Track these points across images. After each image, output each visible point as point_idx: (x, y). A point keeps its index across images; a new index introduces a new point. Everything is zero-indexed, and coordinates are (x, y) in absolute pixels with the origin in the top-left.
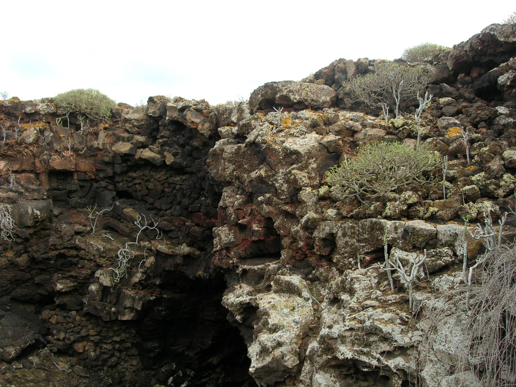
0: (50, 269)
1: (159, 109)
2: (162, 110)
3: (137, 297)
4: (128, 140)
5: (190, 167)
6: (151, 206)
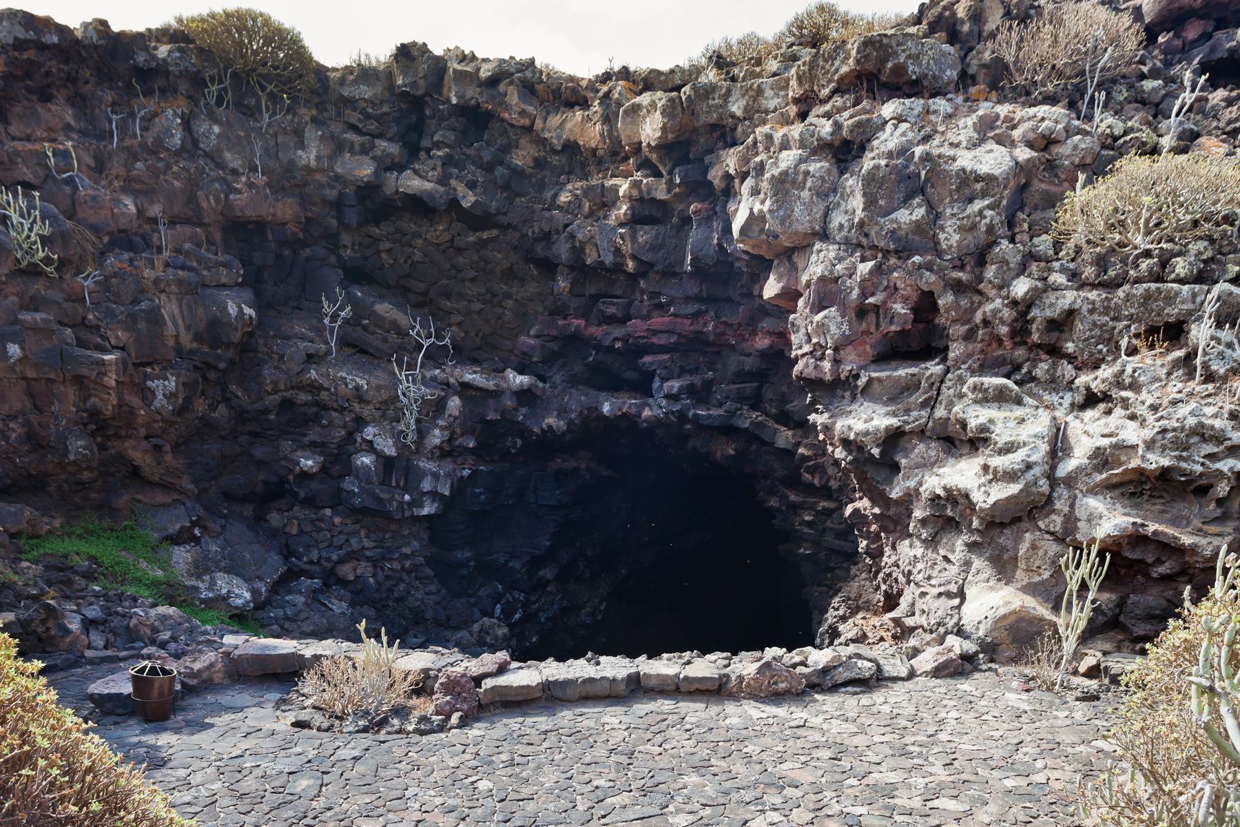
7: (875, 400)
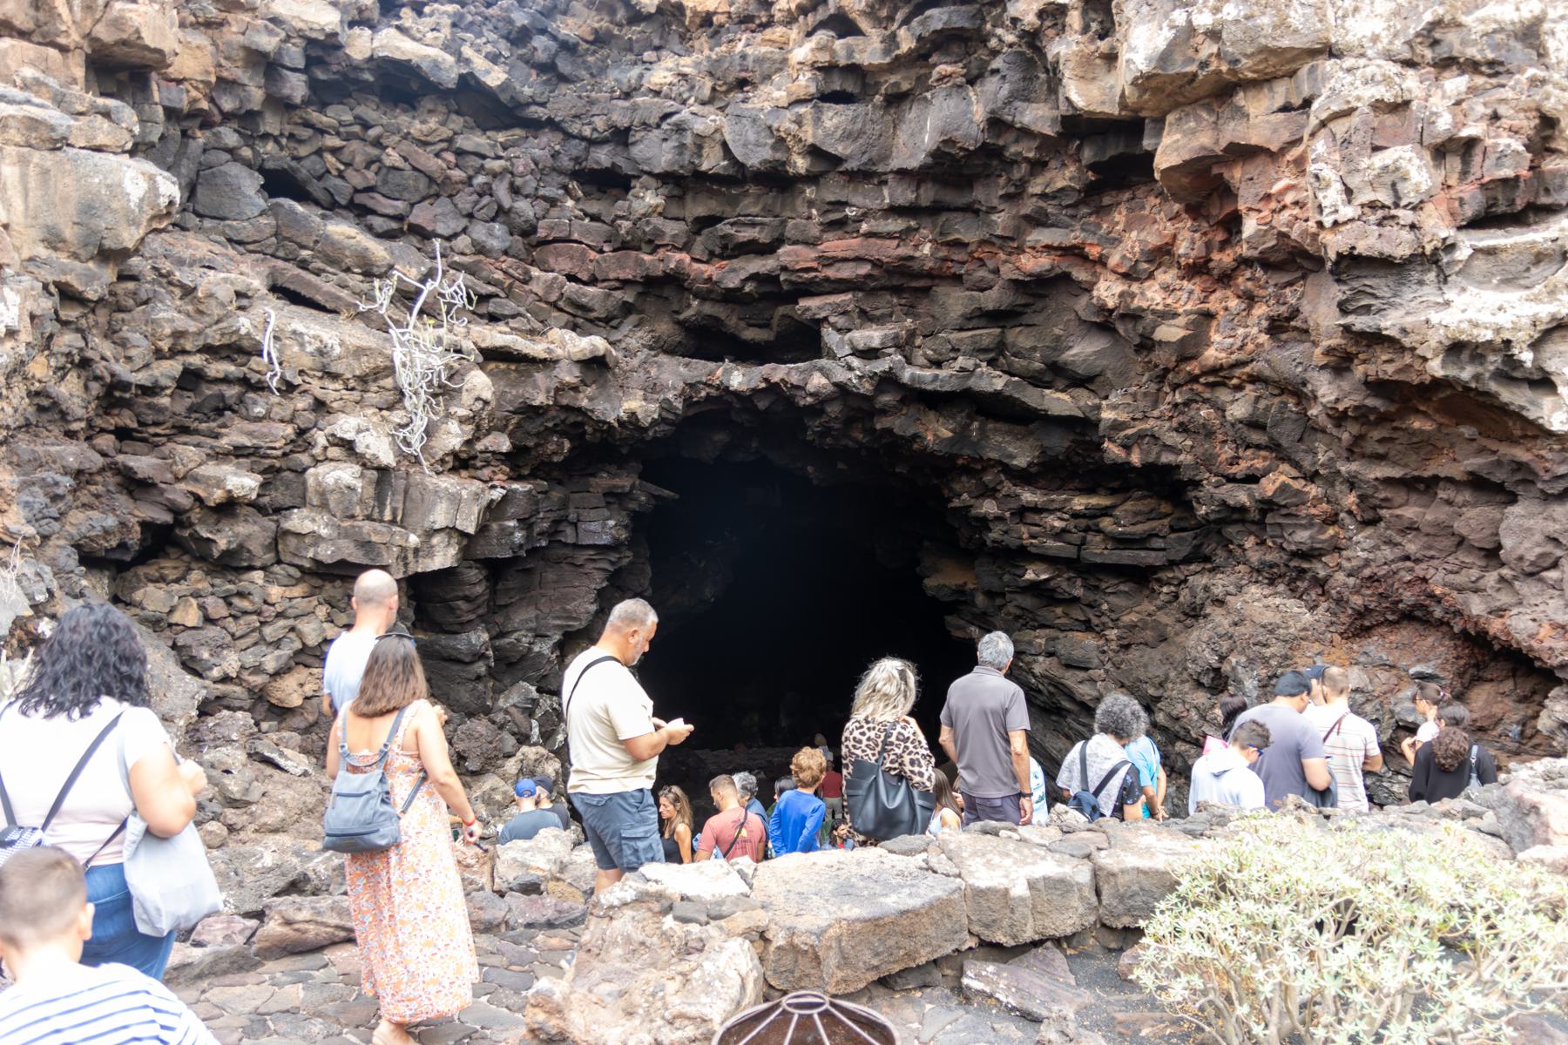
0: (152, 430)
3: (464, 493)
5: (543, 105)
6: (394, 225)
7: (1483, 282)
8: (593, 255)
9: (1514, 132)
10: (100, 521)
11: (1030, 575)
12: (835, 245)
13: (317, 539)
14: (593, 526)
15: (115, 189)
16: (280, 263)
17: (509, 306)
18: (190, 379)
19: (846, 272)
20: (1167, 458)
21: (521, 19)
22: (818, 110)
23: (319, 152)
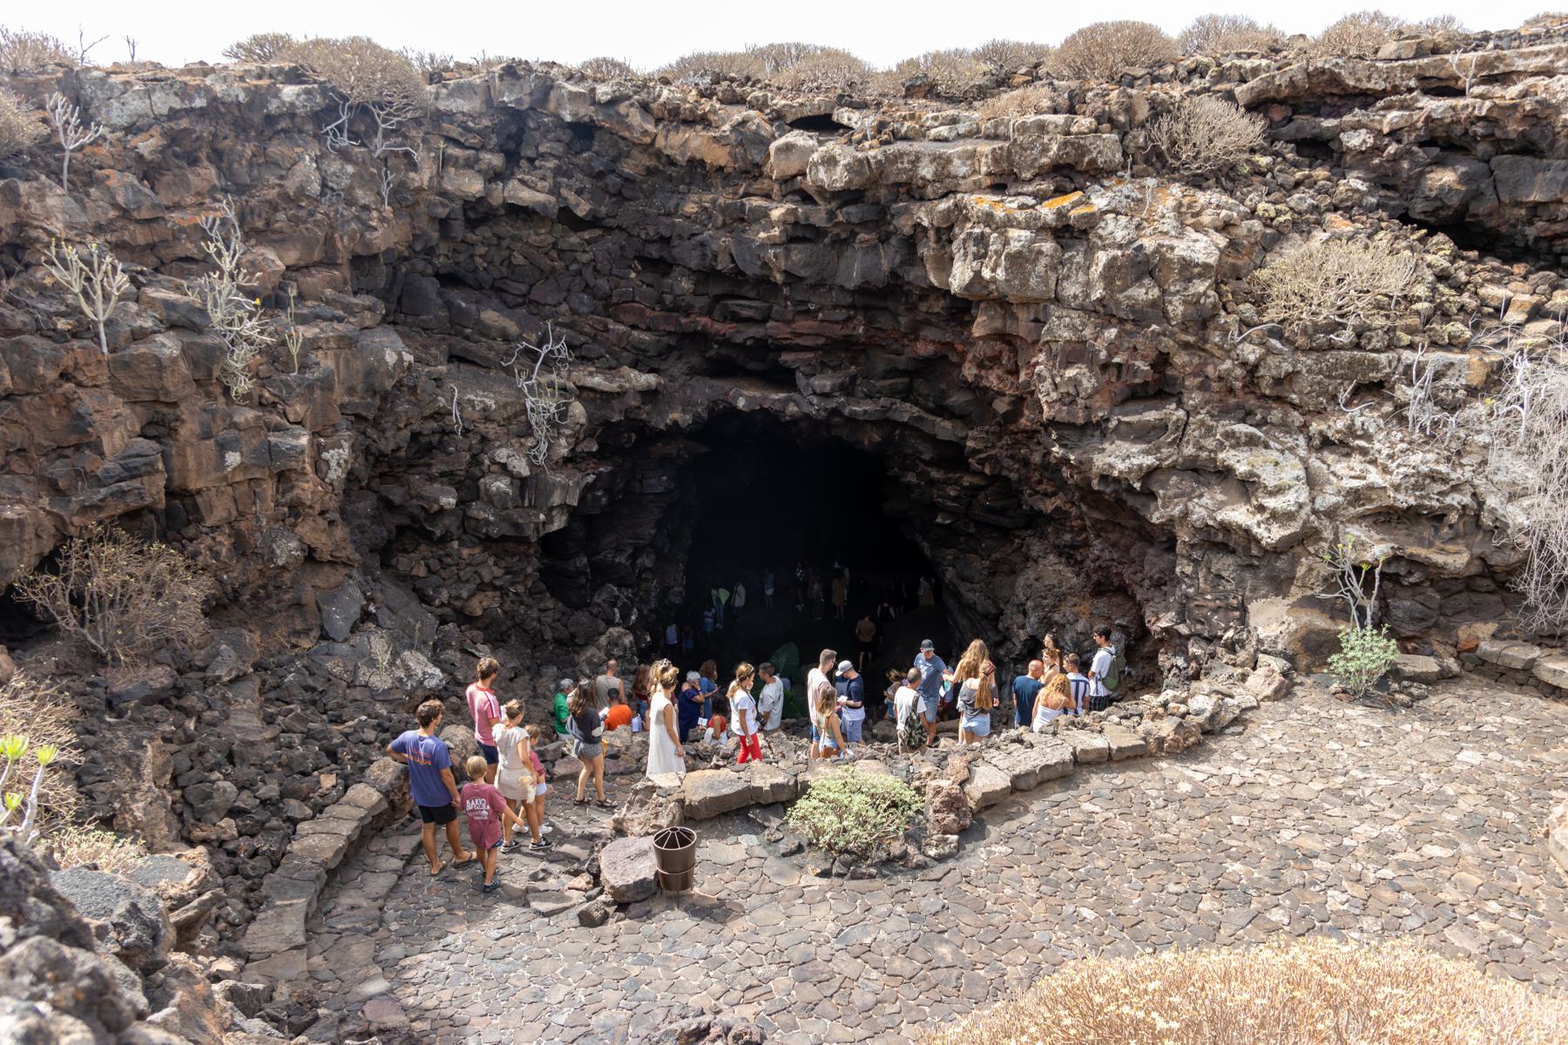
1: (531, 94)
2: (537, 95)
4: (469, 164)
6: (520, 300)
7: (1124, 438)
8: (648, 312)
9: (1144, 358)
10: (382, 533)
11: (939, 520)
12: (803, 325)
13: (487, 523)
14: (653, 481)
15: (382, 361)
16: (453, 340)
17: (597, 349)
18: (415, 436)
19: (808, 342)
20: (1004, 473)
21: (598, 166)
22: (788, 251)
23: (472, 256)
